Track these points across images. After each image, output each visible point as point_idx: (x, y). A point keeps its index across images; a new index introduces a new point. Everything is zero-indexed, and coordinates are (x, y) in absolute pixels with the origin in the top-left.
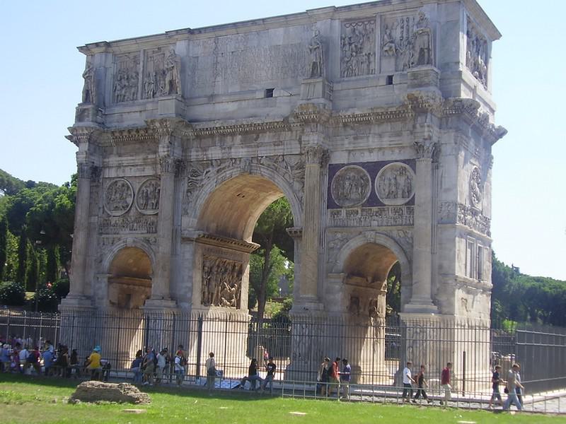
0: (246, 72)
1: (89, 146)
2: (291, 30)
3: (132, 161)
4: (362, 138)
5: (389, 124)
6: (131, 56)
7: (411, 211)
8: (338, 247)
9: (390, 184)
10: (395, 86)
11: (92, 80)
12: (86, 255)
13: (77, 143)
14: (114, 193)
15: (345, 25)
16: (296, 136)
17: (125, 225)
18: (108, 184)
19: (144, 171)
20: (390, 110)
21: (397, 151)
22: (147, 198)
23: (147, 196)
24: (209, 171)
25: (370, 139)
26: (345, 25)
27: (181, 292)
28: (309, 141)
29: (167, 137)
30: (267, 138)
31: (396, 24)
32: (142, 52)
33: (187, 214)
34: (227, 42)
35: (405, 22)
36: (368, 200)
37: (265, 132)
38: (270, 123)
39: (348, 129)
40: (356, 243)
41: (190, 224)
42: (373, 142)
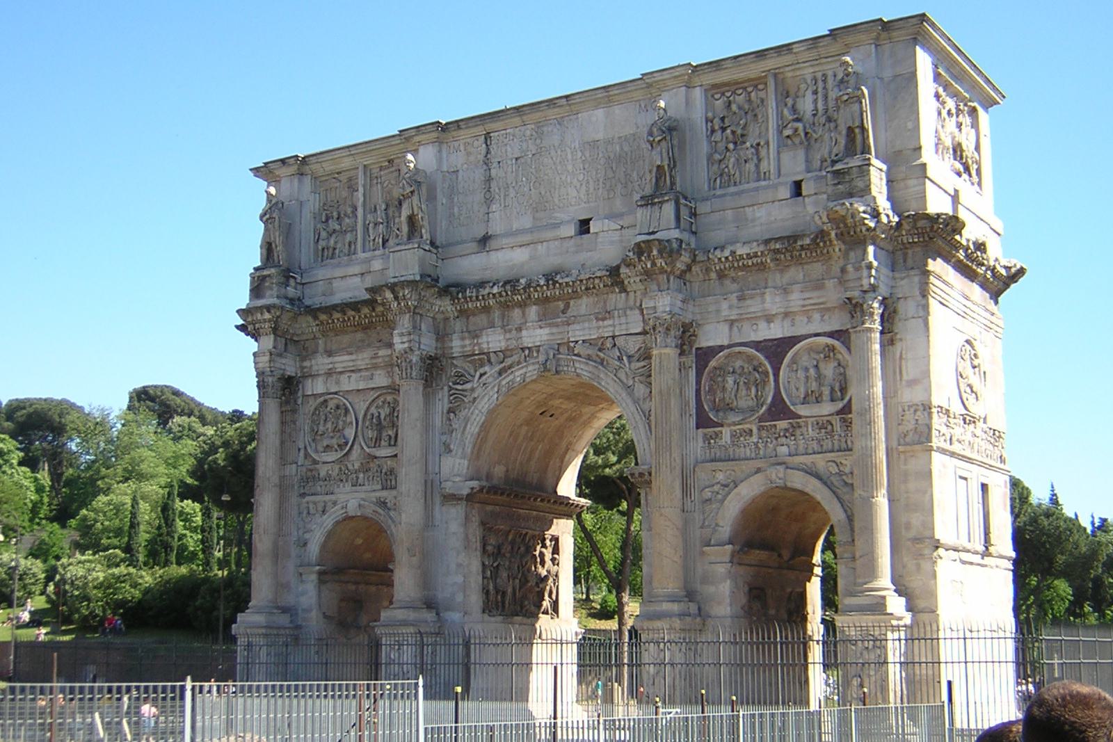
0: (543, 193)
1: (275, 340)
3: (351, 364)
5: (800, 267)
6: (343, 177)
7: (847, 424)
9: (807, 378)
11: (277, 223)
12: (280, 533)
13: (255, 336)
14: (322, 422)
16: (635, 302)
17: (344, 477)
18: (312, 404)
21: (817, 316)
22: (380, 427)
23: (380, 423)
24: (485, 373)
25: (768, 297)
26: (713, 96)
27: (441, 595)
28: (655, 307)
29: (408, 315)
30: (583, 305)
31: (803, 86)
32: (361, 168)
33: (450, 451)
34: (506, 141)
35: (820, 84)
36: (769, 409)
37: (580, 297)
39: (727, 282)
40: (749, 490)
41: (456, 469)
42: (772, 302)
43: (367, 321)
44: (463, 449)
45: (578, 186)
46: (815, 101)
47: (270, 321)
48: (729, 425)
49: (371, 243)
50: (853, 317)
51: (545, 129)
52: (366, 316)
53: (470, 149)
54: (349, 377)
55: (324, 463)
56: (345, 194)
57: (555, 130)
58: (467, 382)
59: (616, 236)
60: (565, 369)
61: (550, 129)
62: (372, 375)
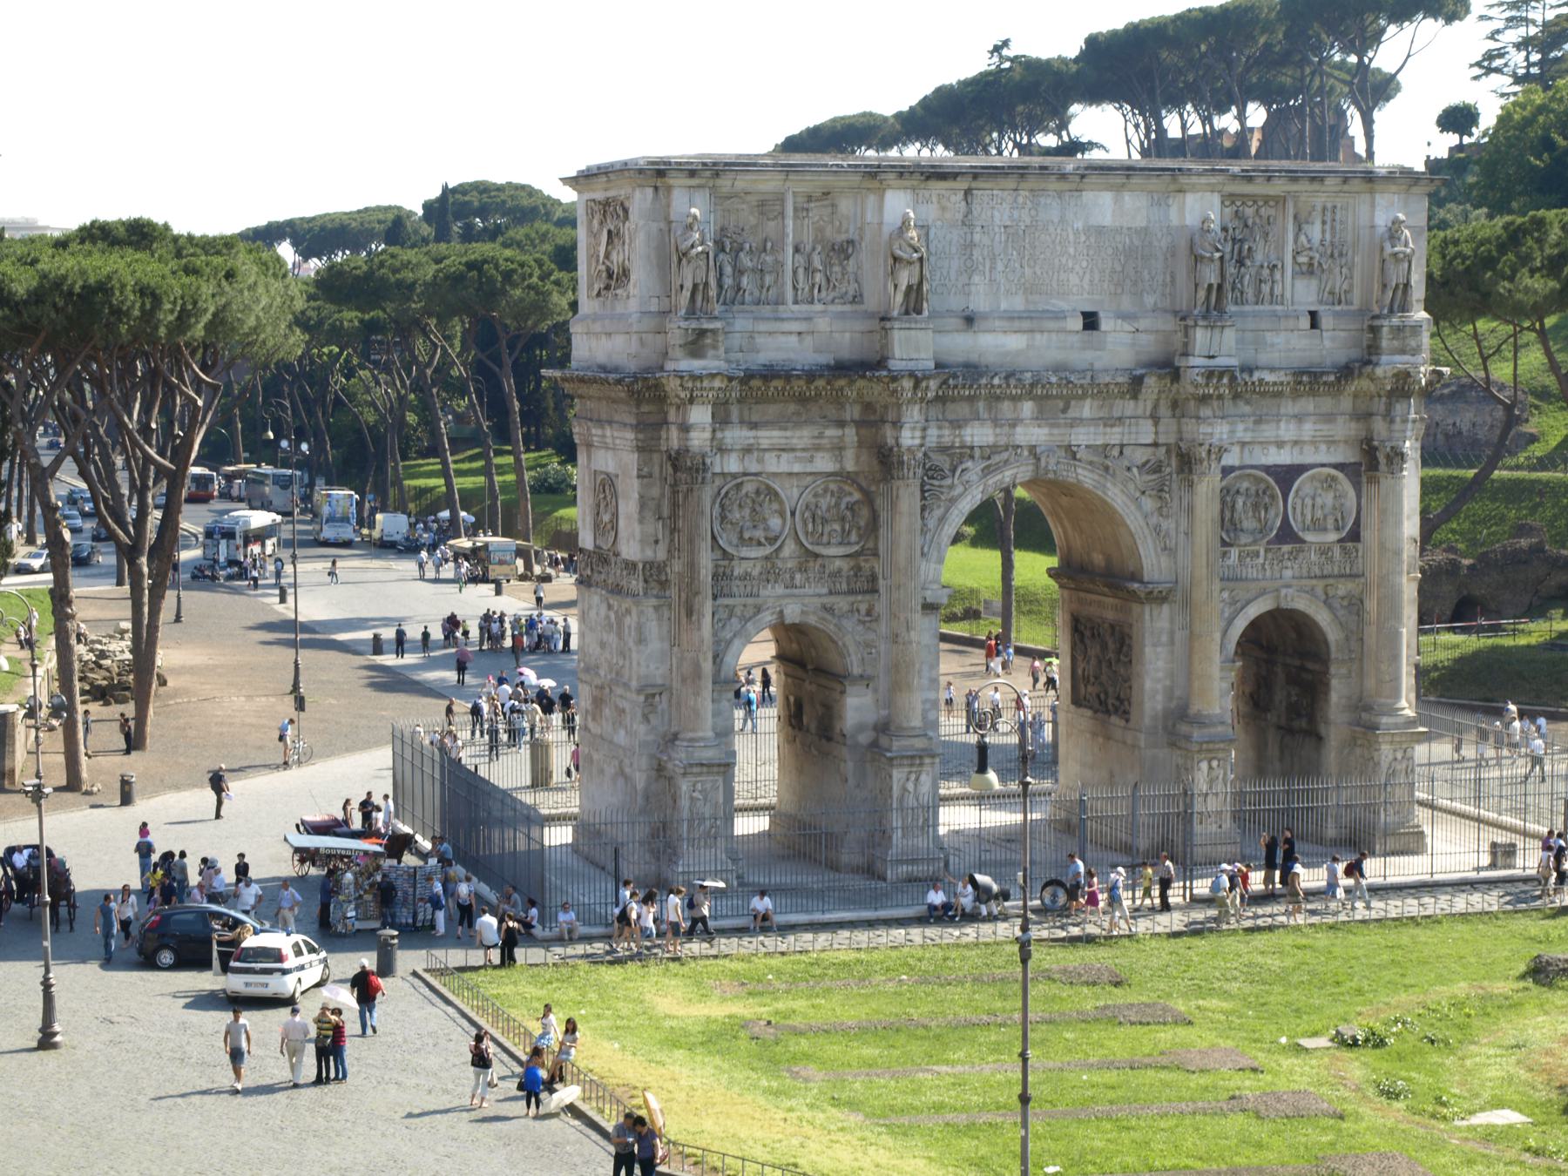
0: (1039, 273)
2: (1127, 198)
3: (783, 441)
4: (1268, 422)
6: (753, 199)
8: (1226, 615)
9: (1313, 506)
10: (1324, 334)
14: (735, 507)
15: (1222, 202)
19: (811, 462)
20: (1325, 378)
21: (1323, 447)
25: (1283, 425)
29: (917, 407)
30: (1087, 409)
35: (1329, 214)
38: (1107, 385)
39: (1241, 403)
42: (1287, 431)
45: (1081, 273)
46: (1323, 232)
47: (720, 389)
48: (1239, 546)
51: (1042, 200)
52: (816, 388)
54: (779, 457)
56: (753, 220)
57: (1054, 204)
58: (943, 478)
59: (1127, 338)
62: (812, 457)
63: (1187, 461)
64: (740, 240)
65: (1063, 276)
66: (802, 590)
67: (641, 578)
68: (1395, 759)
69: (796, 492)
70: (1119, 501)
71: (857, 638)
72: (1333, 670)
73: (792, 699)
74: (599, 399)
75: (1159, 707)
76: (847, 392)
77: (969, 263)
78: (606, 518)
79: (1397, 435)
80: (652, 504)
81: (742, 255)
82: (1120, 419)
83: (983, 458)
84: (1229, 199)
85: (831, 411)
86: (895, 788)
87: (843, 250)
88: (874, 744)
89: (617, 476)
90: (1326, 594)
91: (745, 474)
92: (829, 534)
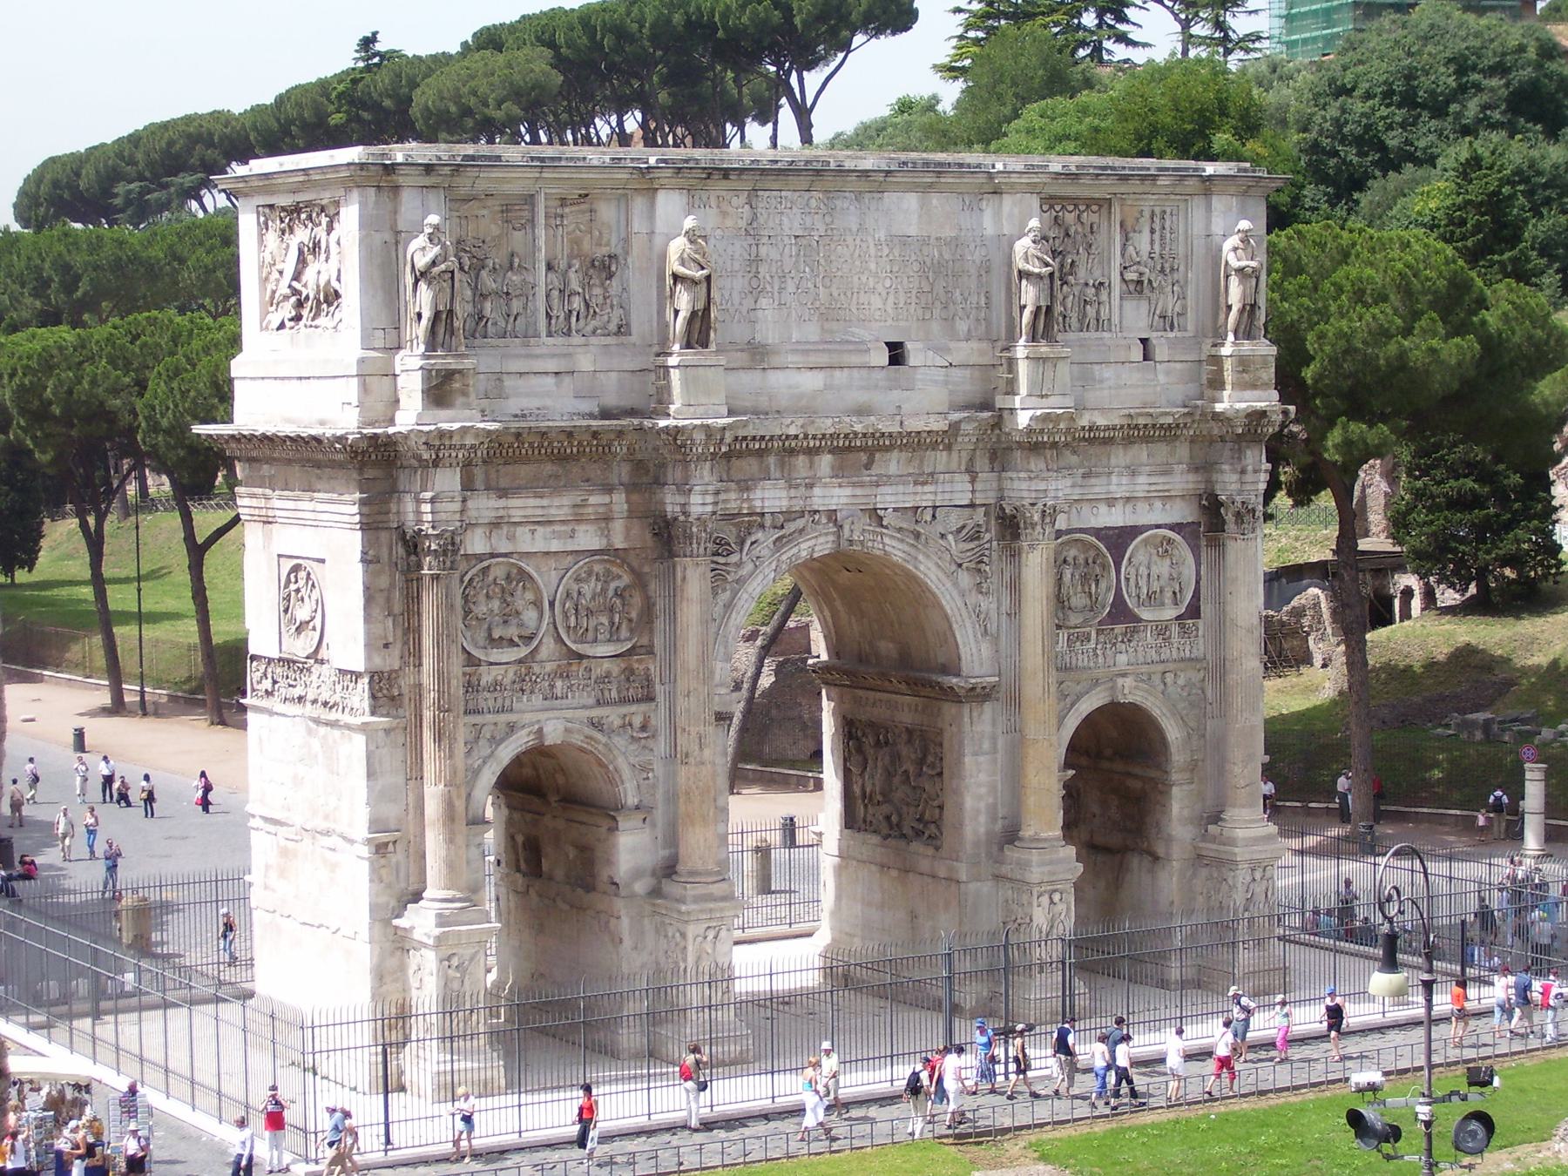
0: (835, 294)
2: (935, 202)
3: (539, 512)
4: (1098, 475)
6: (494, 204)
14: (482, 598)
17: (527, 687)
21: (1158, 504)
25: (1114, 479)
30: (893, 464)
34: (781, 208)
42: (1118, 485)
43: (575, 450)
44: (726, 647)
45: (884, 294)
46: (1152, 242)
49: (553, 321)
50: (1243, 522)
51: (838, 203)
53: (725, 206)
54: (533, 532)
55: (492, 664)
56: (495, 230)
57: (852, 208)
60: (870, 544)
61: (845, 205)
62: (573, 531)
63: (1010, 526)
64: (480, 255)
65: (863, 298)
66: (564, 701)
67: (366, 695)
68: (1254, 880)
69: (554, 576)
70: (934, 578)
71: (632, 760)
72: (1174, 777)
73: (520, 839)
74: (289, 462)
75: (982, 830)
76: (616, 447)
77: (755, 283)
78: (302, 613)
79: (1248, 487)
80: (381, 599)
81: (484, 273)
82: (932, 474)
83: (775, 527)
84: (1049, 201)
85: (595, 471)
86: (690, 948)
87: (605, 267)
88: (656, 892)
89: (322, 561)
90: (1165, 684)
91: (493, 555)
92: (596, 630)
